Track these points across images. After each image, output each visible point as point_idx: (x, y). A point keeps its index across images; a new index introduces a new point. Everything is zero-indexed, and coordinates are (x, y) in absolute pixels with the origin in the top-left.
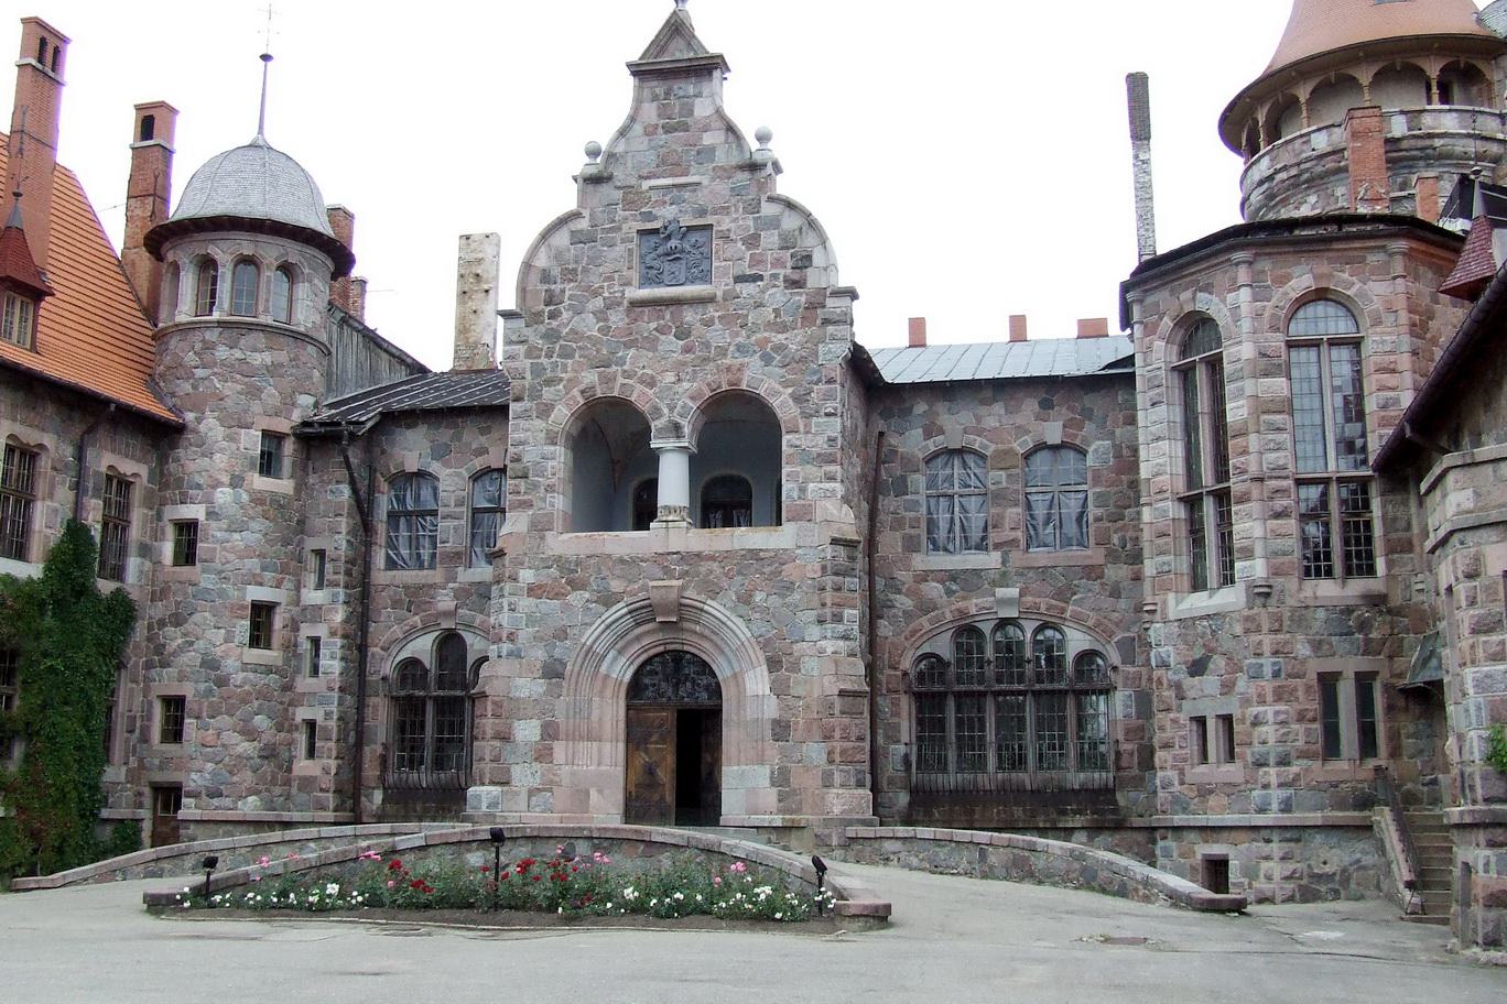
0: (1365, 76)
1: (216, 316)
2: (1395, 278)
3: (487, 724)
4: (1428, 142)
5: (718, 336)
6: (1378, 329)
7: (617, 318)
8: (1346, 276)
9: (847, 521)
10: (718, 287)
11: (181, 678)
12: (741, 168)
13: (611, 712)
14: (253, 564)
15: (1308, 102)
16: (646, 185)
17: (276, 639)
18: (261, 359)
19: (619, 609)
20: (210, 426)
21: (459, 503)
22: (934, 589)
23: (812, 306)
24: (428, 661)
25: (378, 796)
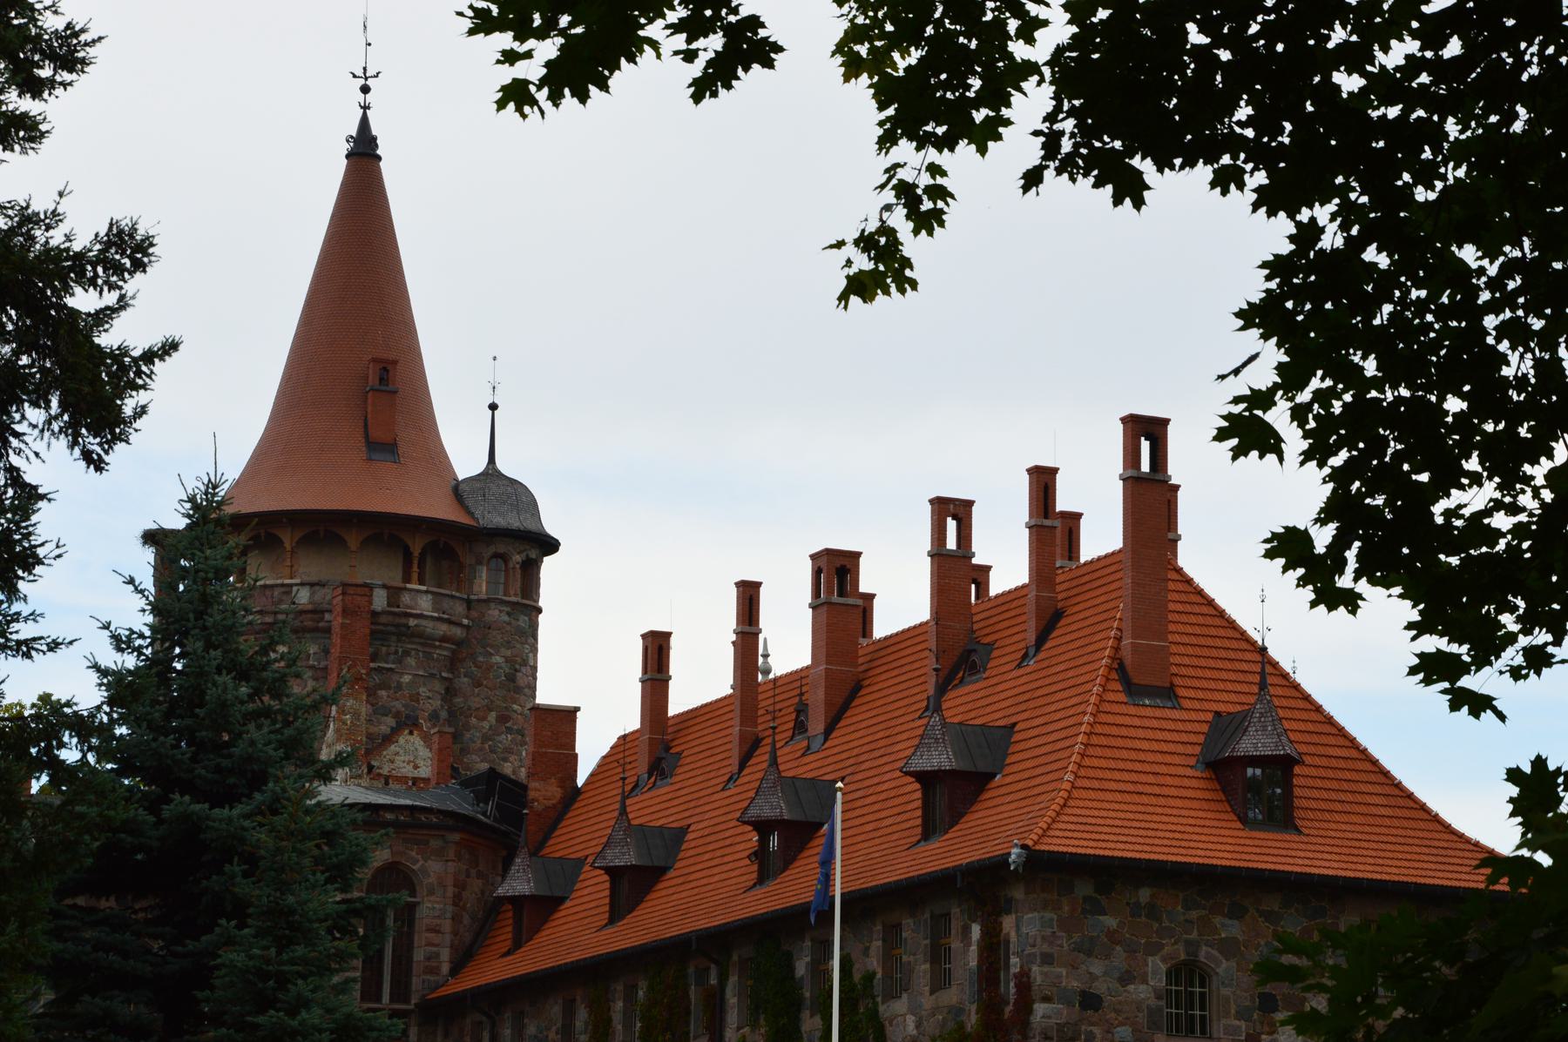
0: (353, 541)
2: (447, 861)
4: (403, 621)
6: (432, 898)
8: (414, 854)
15: (292, 552)
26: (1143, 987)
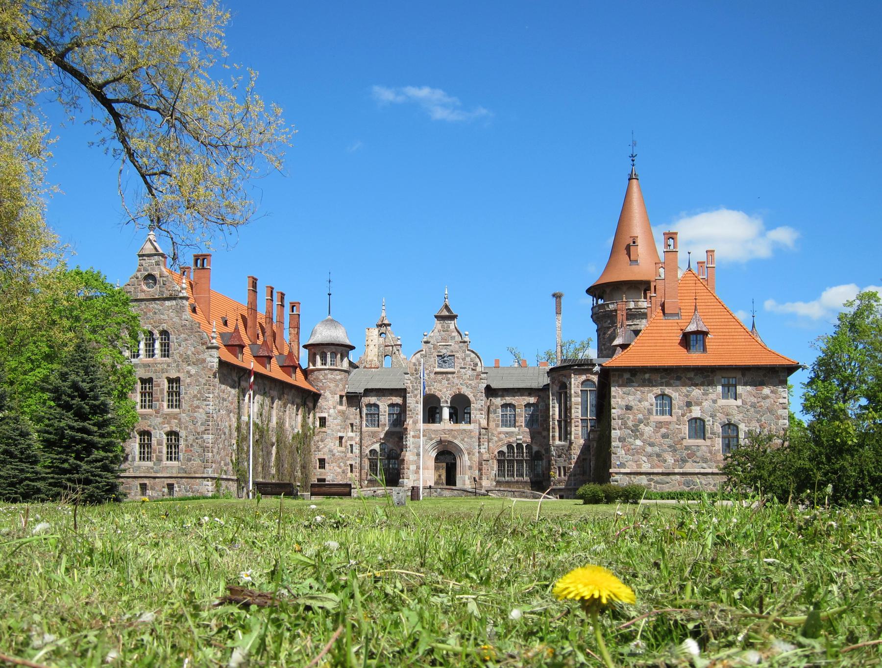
1: (327, 367)
3: (405, 466)
5: (456, 381)
7: (432, 375)
9: (484, 423)
10: (455, 370)
11: (324, 454)
12: (461, 342)
13: (432, 463)
14: (339, 427)
16: (439, 344)
17: (343, 445)
18: (338, 377)
19: (434, 441)
20: (328, 394)
21: (385, 412)
22: (502, 436)
23: (478, 375)
24: (378, 450)
25: (366, 482)
26: (646, 403)
